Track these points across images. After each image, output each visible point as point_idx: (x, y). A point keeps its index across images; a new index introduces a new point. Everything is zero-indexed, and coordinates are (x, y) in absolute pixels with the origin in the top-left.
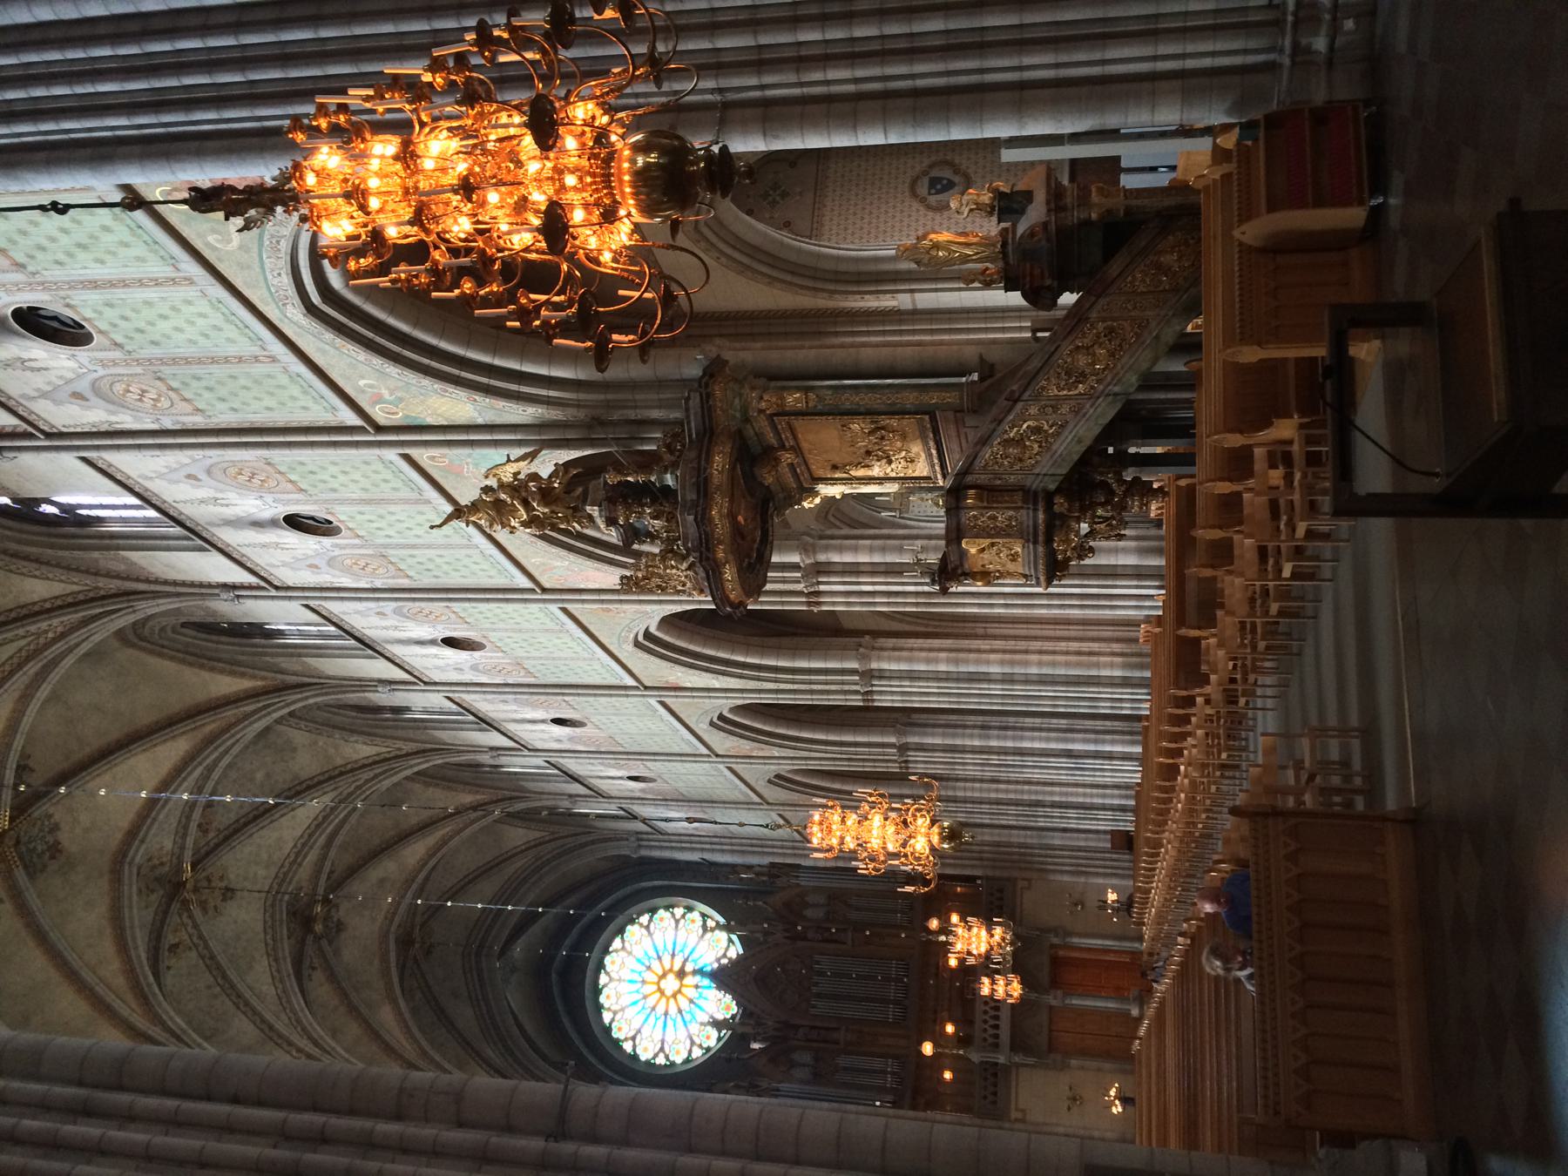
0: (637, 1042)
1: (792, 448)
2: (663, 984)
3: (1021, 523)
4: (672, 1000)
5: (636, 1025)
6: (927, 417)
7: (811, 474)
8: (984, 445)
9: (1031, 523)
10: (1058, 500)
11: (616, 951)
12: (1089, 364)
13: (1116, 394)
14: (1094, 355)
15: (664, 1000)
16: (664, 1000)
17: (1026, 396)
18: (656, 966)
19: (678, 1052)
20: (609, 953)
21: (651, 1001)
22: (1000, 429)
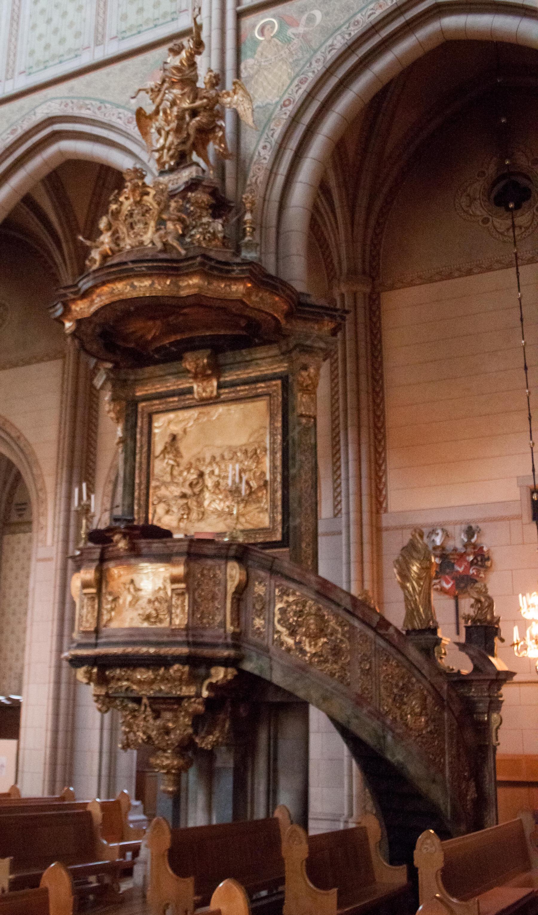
1: (218, 395)
3: (204, 628)
6: (278, 537)
7: (158, 412)
8: (318, 592)
9: (206, 640)
10: (231, 672)
12: (413, 709)
13: (384, 737)
14: (421, 715)
17: (381, 643)
22: (341, 612)
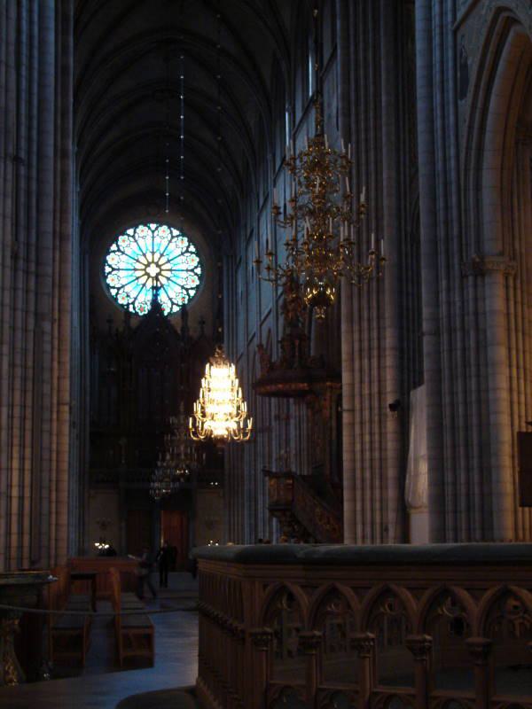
0: (117, 253)
2: (153, 266)
4: (143, 272)
5: (127, 251)
11: (171, 232)
15: (143, 267)
16: (143, 267)
18: (163, 260)
19: (113, 280)
20: (169, 228)
21: (142, 259)
